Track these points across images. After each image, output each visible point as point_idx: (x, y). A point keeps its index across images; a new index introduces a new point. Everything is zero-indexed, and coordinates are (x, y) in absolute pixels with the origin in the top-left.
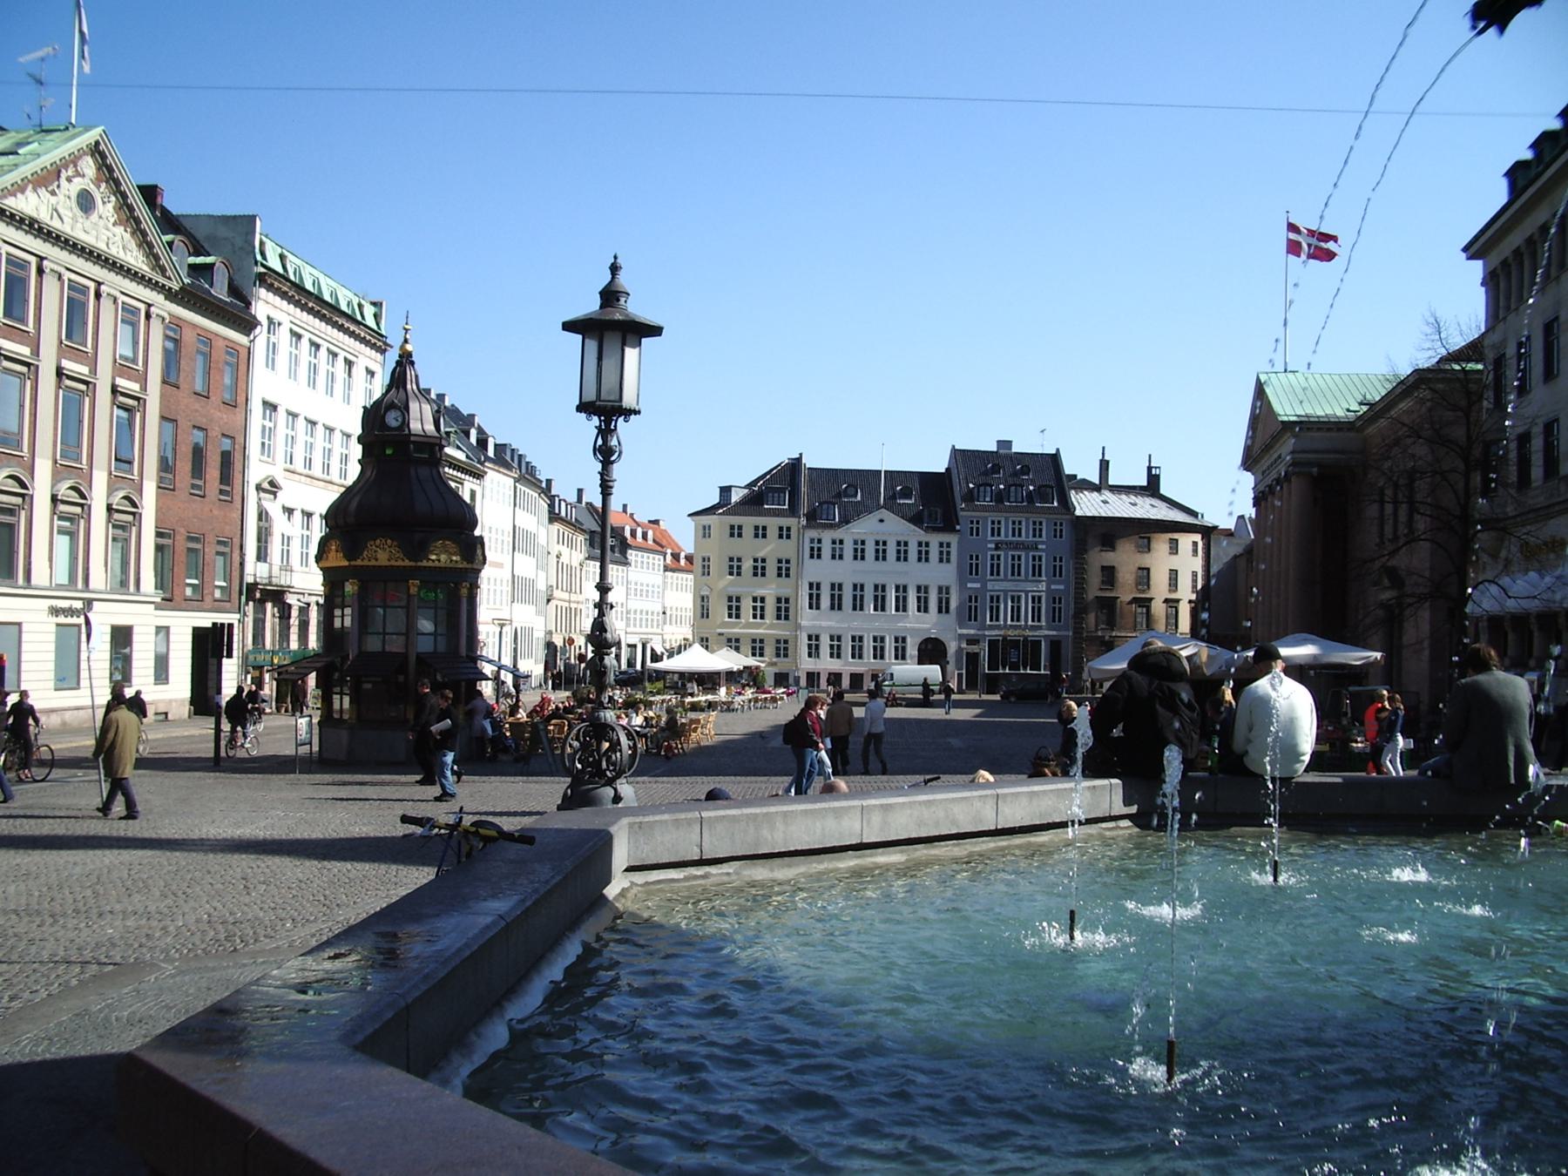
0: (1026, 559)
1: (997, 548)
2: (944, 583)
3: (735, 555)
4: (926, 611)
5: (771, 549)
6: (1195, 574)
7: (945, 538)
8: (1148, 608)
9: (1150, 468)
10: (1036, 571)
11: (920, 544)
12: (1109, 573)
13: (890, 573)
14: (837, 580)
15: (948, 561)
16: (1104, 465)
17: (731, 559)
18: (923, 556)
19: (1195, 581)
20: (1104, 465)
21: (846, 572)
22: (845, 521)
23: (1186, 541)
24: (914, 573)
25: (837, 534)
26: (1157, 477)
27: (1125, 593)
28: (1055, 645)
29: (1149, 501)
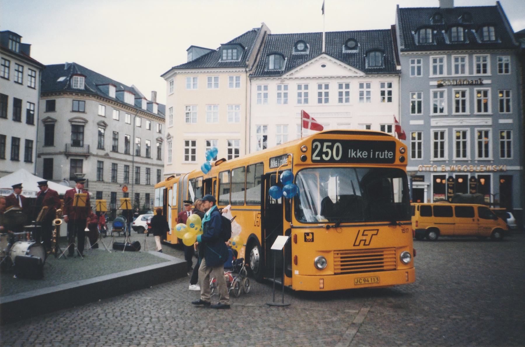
0: (472, 96)
1: (440, 86)
7: (387, 80)
10: (482, 106)
11: (361, 86)
15: (390, 100)
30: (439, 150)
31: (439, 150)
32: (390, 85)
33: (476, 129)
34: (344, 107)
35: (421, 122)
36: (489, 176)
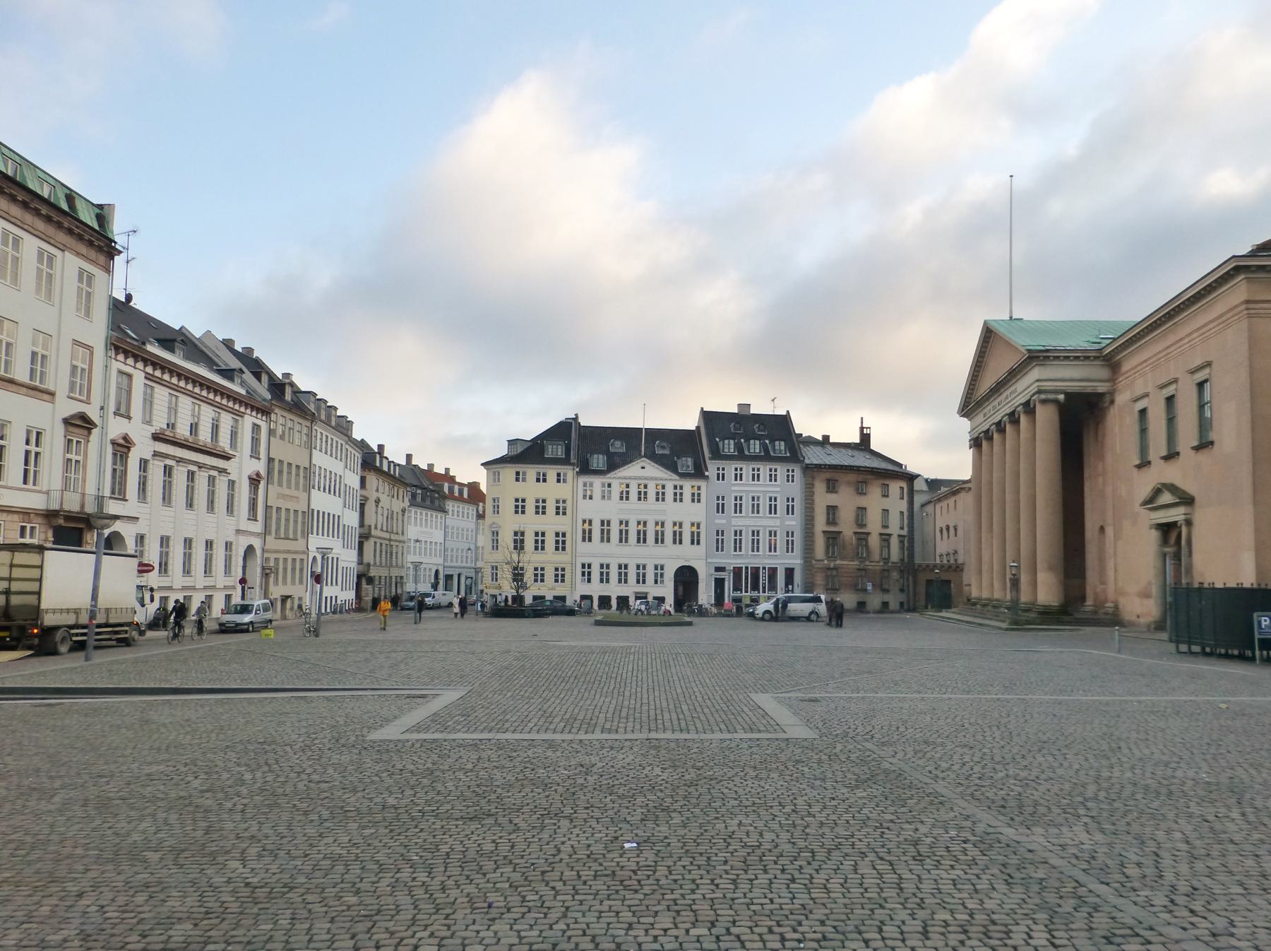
2: (696, 520)
3: (520, 496)
5: (552, 491)
6: (902, 513)
7: (696, 483)
9: (862, 429)
11: (675, 487)
12: (832, 510)
13: (650, 511)
14: (606, 518)
15: (699, 501)
17: (517, 500)
18: (678, 497)
21: (612, 510)
22: (612, 466)
23: (895, 487)
24: (672, 512)
25: (606, 479)
26: (869, 435)
28: (790, 573)
29: (862, 454)
30: (738, 546)
31: (738, 546)
32: (699, 488)
34: (660, 505)
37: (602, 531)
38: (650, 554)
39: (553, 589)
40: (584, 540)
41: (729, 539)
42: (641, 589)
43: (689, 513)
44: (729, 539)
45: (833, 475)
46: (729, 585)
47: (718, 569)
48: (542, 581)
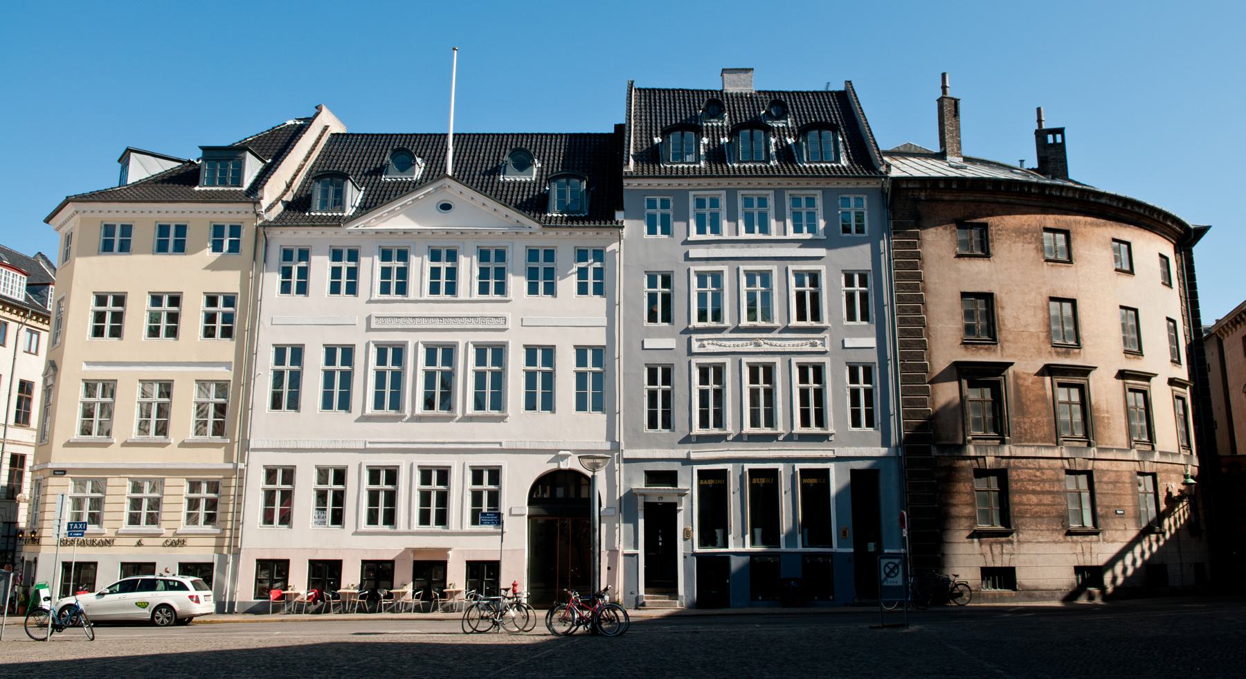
4: (549, 405)
5: (196, 274)
8: (1083, 390)
9: (1041, 134)
16: (948, 110)
19: (1174, 340)
20: (948, 110)
27: (1023, 352)
33: (795, 360)
35: (670, 343)
36: (827, 471)
37: (329, 377)
38: (459, 440)
39: (178, 542)
40: (276, 404)
41: (688, 392)
42: (429, 540)
43: (566, 318)
44: (688, 392)
45: (971, 205)
46: (687, 519)
47: (654, 477)
48: (152, 520)
